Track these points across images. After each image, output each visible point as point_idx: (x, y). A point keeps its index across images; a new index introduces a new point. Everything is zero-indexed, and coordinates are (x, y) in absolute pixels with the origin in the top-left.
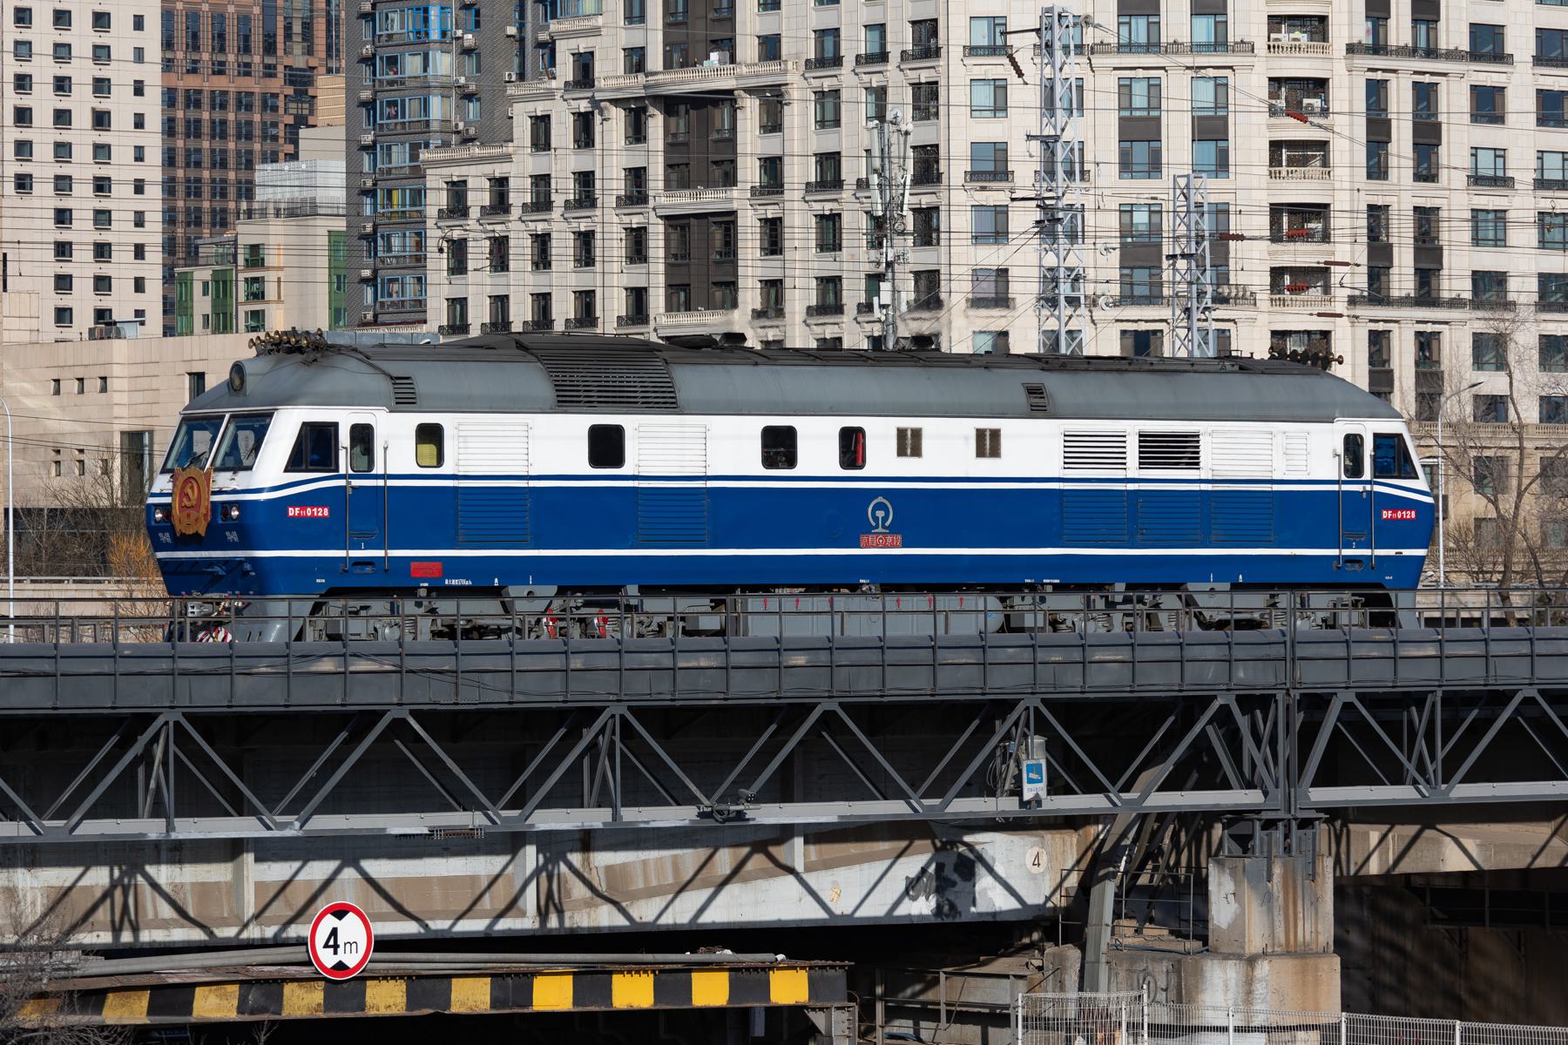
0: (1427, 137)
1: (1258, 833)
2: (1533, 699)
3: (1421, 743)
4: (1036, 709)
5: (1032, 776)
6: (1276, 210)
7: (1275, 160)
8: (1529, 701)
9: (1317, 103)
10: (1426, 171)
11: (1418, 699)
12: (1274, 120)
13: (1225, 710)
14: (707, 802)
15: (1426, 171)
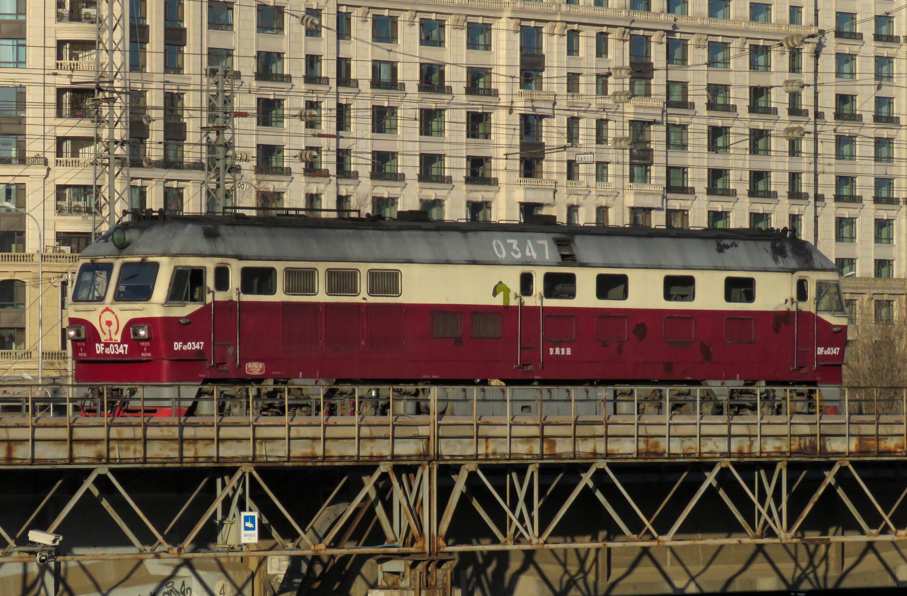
0: (175, 37)
1: (408, 573)
2: (603, 470)
3: (521, 505)
4: (251, 475)
5: (249, 525)
6: (60, 92)
7: (59, 56)
8: (600, 473)
9: (92, 11)
10: (172, 65)
11: (521, 470)
12: (61, 25)
13: (384, 476)
14: (12, 543)
15: (172, 65)
